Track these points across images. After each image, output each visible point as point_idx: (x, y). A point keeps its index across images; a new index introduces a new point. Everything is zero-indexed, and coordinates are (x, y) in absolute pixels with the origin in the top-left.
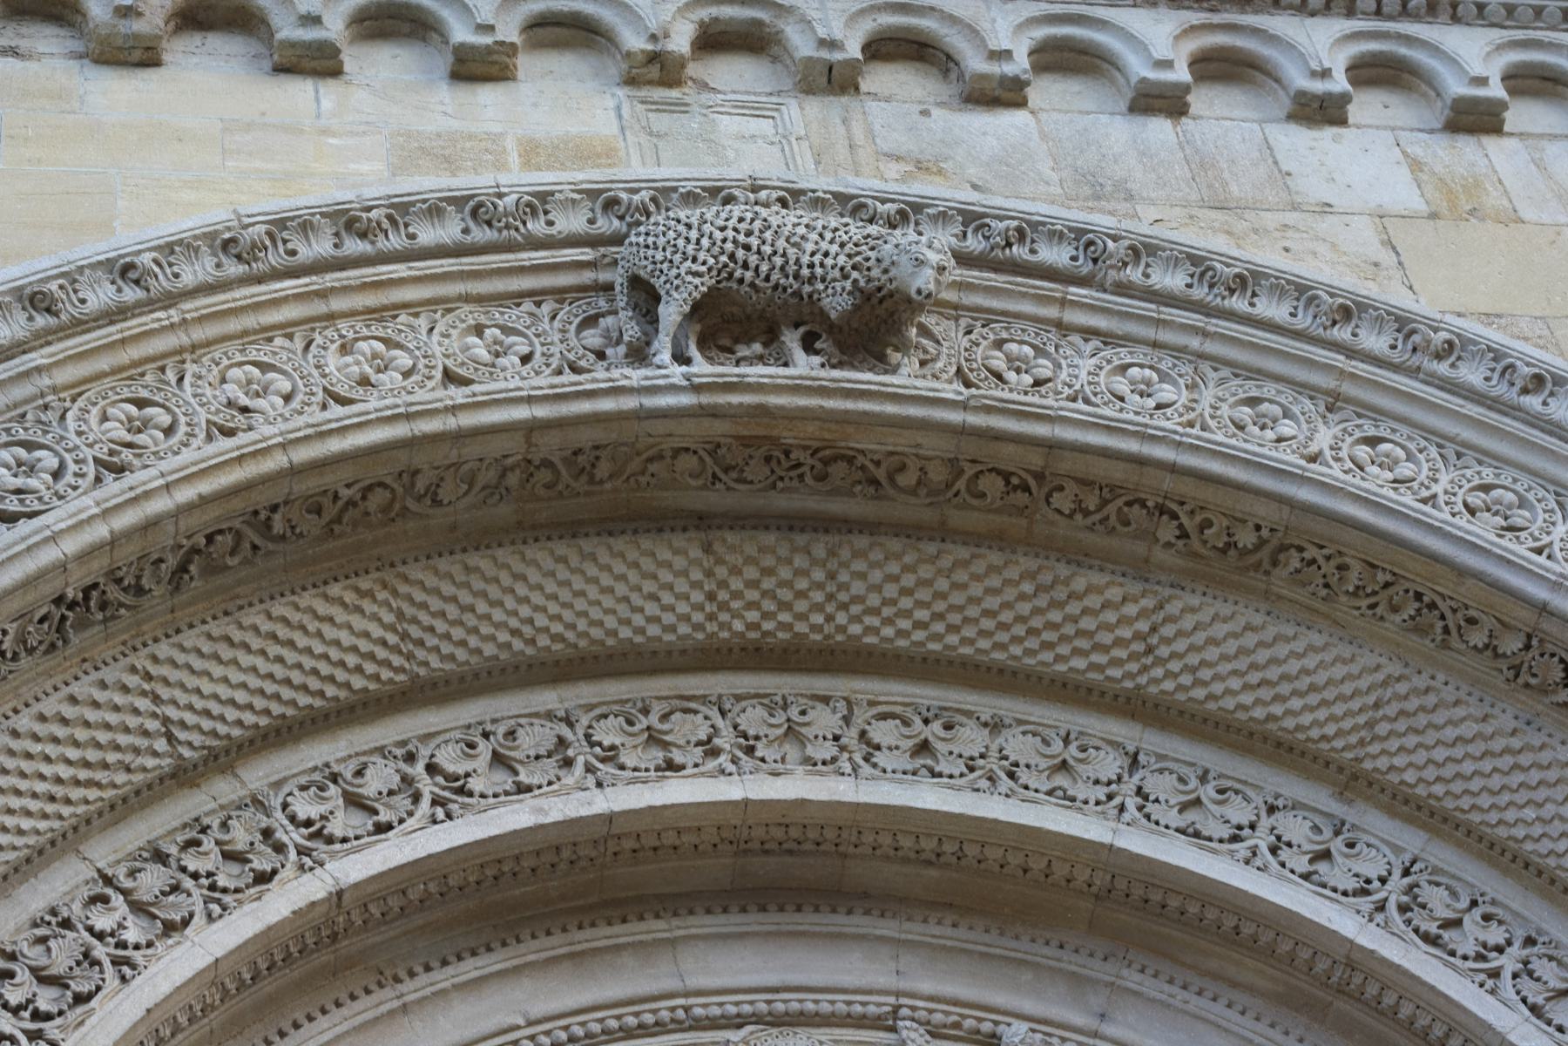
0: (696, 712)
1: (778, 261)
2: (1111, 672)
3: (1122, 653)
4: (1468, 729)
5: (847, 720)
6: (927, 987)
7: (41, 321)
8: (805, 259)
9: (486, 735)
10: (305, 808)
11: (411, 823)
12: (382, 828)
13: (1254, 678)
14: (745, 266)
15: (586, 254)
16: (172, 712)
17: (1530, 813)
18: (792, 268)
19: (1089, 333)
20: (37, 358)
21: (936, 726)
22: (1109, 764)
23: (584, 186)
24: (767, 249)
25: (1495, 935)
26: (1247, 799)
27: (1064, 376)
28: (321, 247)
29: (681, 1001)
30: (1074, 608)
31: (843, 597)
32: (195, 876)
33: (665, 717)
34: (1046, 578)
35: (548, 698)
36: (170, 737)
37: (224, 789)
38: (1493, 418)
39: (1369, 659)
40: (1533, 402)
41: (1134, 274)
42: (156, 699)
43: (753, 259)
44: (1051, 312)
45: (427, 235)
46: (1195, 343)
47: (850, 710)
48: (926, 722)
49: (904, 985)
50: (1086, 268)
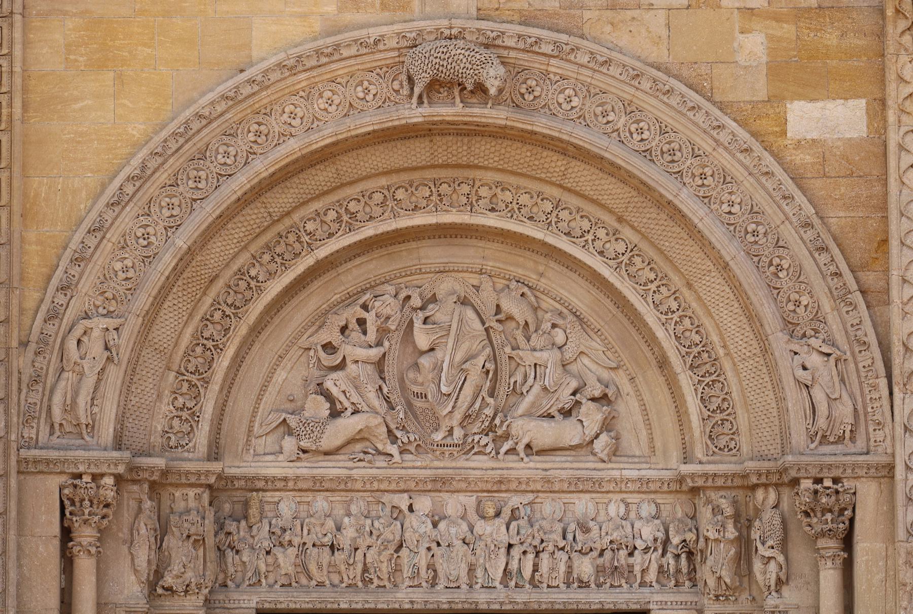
0: (426, 185)
1: (452, 71)
2: (552, 179)
3: (556, 175)
4: (654, 215)
5: (473, 186)
7: (230, 103)
8: (460, 71)
9: (363, 196)
10: (310, 226)
11: (340, 233)
12: (331, 235)
13: (594, 188)
14: (442, 72)
15: (396, 53)
16: (271, 210)
17: (667, 244)
18: (456, 73)
19: (555, 74)
20: (228, 116)
21: (499, 189)
22: (548, 206)
23: (396, 31)
24: (449, 67)
25: (652, 276)
26: (590, 221)
27: (543, 96)
28: (313, 62)
29: (419, 267)
30: (542, 161)
31: (473, 153)
32: (278, 255)
35: (383, 181)
36: (270, 216)
37: (287, 222)
38: (677, 116)
40: (690, 114)
41: (572, 57)
42: (266, 207)
43: (444, 71)
45: (346, 53)
47: (474, 183)
48: (497, 187)
49: (484, 263)
50: (555, 53)
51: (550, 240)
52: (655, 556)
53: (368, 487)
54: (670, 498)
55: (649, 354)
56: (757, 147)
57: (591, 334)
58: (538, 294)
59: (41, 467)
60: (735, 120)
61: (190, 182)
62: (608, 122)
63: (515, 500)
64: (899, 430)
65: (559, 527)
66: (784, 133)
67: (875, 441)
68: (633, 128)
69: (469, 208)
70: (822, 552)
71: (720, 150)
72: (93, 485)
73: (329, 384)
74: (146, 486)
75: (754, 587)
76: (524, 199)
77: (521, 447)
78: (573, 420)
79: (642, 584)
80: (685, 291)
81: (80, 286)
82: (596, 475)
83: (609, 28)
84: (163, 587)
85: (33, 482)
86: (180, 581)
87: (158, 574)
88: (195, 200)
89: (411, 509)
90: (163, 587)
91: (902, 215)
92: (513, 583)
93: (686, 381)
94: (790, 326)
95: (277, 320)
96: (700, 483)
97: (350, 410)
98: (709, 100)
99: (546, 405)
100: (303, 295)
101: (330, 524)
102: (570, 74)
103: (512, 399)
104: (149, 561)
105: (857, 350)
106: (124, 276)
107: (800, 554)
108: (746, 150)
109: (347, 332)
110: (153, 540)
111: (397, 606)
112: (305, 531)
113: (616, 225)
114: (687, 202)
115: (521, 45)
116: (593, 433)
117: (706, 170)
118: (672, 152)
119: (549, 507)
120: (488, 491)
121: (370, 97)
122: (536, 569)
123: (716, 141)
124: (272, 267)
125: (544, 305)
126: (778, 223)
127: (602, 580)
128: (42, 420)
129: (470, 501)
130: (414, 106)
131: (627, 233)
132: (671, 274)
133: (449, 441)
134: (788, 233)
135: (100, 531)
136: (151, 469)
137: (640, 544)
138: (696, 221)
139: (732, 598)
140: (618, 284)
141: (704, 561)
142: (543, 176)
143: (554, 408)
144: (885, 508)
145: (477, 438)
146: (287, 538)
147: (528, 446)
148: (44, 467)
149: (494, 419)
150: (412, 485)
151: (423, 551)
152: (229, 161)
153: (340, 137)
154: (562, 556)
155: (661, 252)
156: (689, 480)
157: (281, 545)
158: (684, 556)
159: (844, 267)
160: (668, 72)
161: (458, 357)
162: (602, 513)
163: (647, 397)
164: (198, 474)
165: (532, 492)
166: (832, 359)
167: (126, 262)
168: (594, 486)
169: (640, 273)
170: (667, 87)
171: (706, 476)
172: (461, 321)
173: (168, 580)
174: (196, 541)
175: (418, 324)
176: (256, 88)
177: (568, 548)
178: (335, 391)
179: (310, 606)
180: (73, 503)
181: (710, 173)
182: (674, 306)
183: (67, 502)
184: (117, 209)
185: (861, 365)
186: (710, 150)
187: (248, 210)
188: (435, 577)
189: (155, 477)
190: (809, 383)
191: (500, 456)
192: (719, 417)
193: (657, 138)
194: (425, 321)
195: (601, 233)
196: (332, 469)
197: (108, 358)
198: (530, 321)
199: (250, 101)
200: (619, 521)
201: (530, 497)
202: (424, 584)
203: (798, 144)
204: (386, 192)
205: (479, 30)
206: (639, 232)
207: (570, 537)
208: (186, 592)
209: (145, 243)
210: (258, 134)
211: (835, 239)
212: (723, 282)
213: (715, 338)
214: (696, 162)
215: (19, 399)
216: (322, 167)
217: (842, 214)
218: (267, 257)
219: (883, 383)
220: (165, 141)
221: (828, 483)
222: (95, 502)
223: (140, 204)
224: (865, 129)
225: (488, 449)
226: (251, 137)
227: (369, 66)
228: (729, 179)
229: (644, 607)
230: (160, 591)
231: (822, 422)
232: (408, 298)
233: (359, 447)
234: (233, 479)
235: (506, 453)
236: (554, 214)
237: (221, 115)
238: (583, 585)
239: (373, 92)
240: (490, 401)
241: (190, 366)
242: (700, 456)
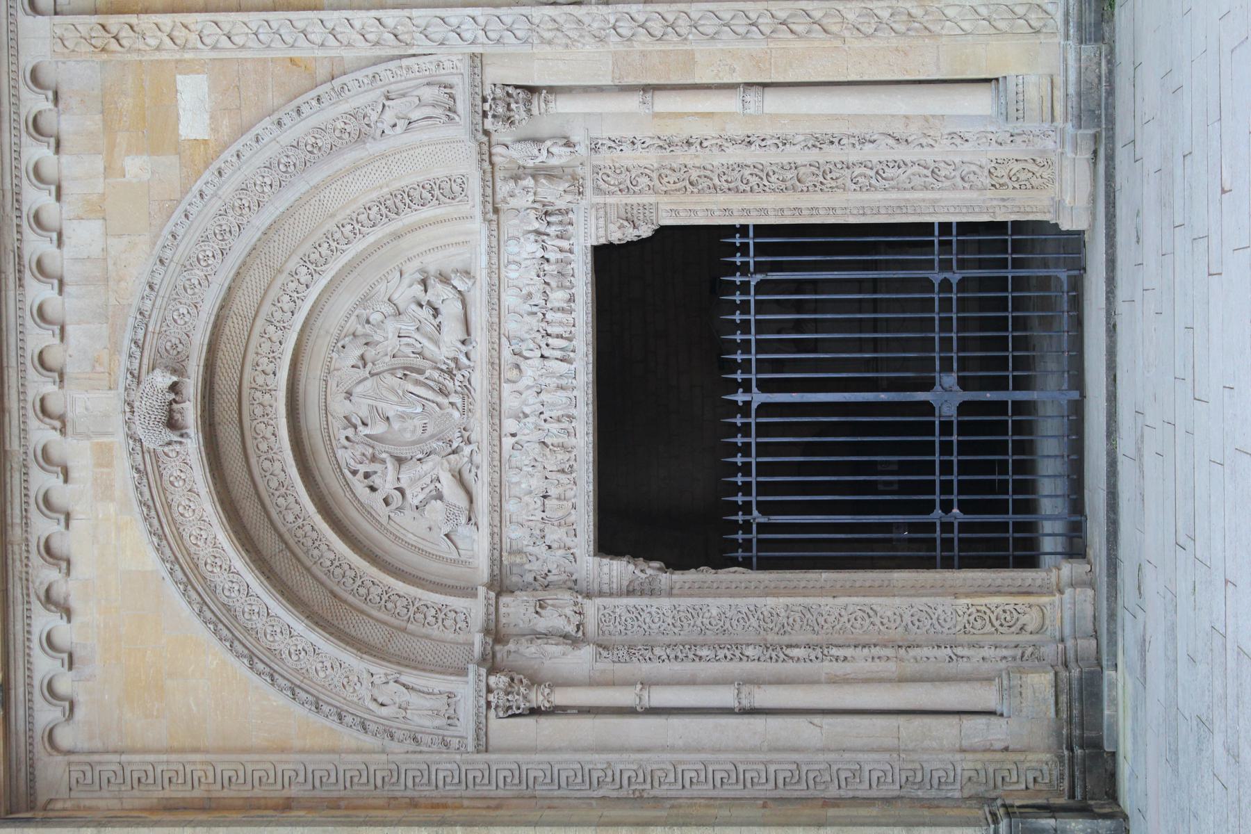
6: (319, 373)
10: (291, 518)
12: (297, 502)
19: (161, 326)
20: (200, 589)
25: (326, 245)
28: (155, 522)
33: (258, 434)
34: (227, 341)
35: (253, 460)
37: (287, 536)
39: (255, 266)
40: (191, 218)
44: (156, 336)
45: (147, 495)
46: (166, 299)
51: (298, 327)
52: (549, 242)
53: (497, 469)
54: (504, 228)
55: (389, 247)
56: (218, 164)
57: (373, 292)
58: (343, 335)
59: (482, 733)
60: (196, 181)
61: (254, 618)
62: (200, 284)
63: (506, 353)
64: (443, 49)
65: (527, 319)
66: (205, 142)
68: (204, 264)
69: (273, 392)
70: (542, 111)
71: (220, 193)
72: (496, 692)
73: (416, 502)
74: (498, 648)
75: (572, 164)
76: (266, 347)
77: (464, 349)
78: (442, 308)
79: (571, 252)
80: (336, 220)
81: (338, 704)
82: (485, 288)
83: (123, 284)
84: (577, 632)
85: (493, 742)
86: (572, 619)
87: (566, 636)
88: (268, 614)
89: (513, 435)
90: (577, 632)
91: (269, 47)
92: (572, 354)
93: (408, 218)
94: (361, 137)
95: (367, 542)
96: (490, 207)
97: (437, 484)
98: (179, 202)
99: (430, 329)
100: (346, 522)
101: (526, 499)
102: (161, 315)
103: (427, 354)
104: (556, 644)
105: (379, 83)
106: (330, 669)
107: (545, 127)
108: (220, 173)
109: (375, 486)
110: (539, 641)
111: (591, 446)
112: (533, 518)
113: (285, 274)
114: (262, 220)
115: (138, 354)
116: (453, 291)
117: (236, 204)
118: (223, 232)
119: (511, 326)
120: (500, 374)
121: (183, 475)
122: (559, 336)
123: (213, 196)
124: (324, 547)
125: (351, 331)
126: (278, 146)
127: (568, 284)
128: (446, 733)
129: (506, 387)
130: (189, 441)
131: (292, 265)
132: (324, 230)
133: (460, 405)
134: (288, 137)
135: (533, 684)
136: (484, 644)
137: (540, 253)
138: (278, 213)
139: (581, 181)
140: (333, 273)
141: (552, 204)
142: (246, 333)
143: (433, 322)
145: (457, 383)
146: (538, 532)
147: (463, 342)
148: (482, 733)
149: (442, 370)
150: (496, 434)
151: (546, 426)
152: (237, 588)
153: (216, 499)
154: (549, 316)
155: (305, 238)
156: (488, 216)
157: (544, 537)
158: (548, 219)
159: (314, 93)
160: (157, 236)
161: (395, 399)
162: (515, 283)
163: (423, 248)
164: (488, 605)
165: (499, 339)
166: (387, 103)
167: (319, 668)
168: (495, 290)
169: (323, 255)
170: (170, 237)
171: (484, 203)
172: (364, 396)
173: (571, 629)
174: (541, 606)
175: (367, 431)
176: (177, 567)
177: (544, 311)
178: (421, 497)
179: (591, 514)
180: (510, 708)
181: (239, 201)
182: (350, 227)
183: (510, 712)
184: (276, 676)
185: (392, 80)
186: (220, 203)
187: (277, 570)
188: (569, 416)
189: (490, 640)
190: (407, 122)
191: (472, 364)
192: (437, 192)
193: (211, 244)
194: (365, 424)
195: (293, 286)
196: (483, 497)
197: (396, 682)
198: (365, 341)
199: (188, 571)
200: (522, 270)
201: (504, 340)
202: (573, 424)
203: (214, 130)
204: (262, 458)
205: (126, 389)
206: (290, 256)
207: (535, 309)
208: (580, 613)
209: (303, 653)
210: (214, 564)
211: (291, 100)
212: (328, 189)
213: (374, 195)
214: (230, 211)
215: (427, 752)
216: (241, 511)
217: (270, 95)
218: (316, 552)
219: (405, 62)
220: (221, 639)
221: (487, 107)
222: (510, 689)
223: (272, 658)
224: (201, 76)
225: (466, 374)
226: (217, 570)
227: (157, 476)
228: (244, 186)
229: (589, 249)
230: (580, 634)
231: (438, 112)
232: (347, 438)
233: (466, 475)
234: (492, 576)
235: (469, 359)
236: (278, 324)
237: (199, 595)
238: (572, 299)
239: (179, 473)
240: (427, 374)
241: (401, 614)
242: (468, 207)
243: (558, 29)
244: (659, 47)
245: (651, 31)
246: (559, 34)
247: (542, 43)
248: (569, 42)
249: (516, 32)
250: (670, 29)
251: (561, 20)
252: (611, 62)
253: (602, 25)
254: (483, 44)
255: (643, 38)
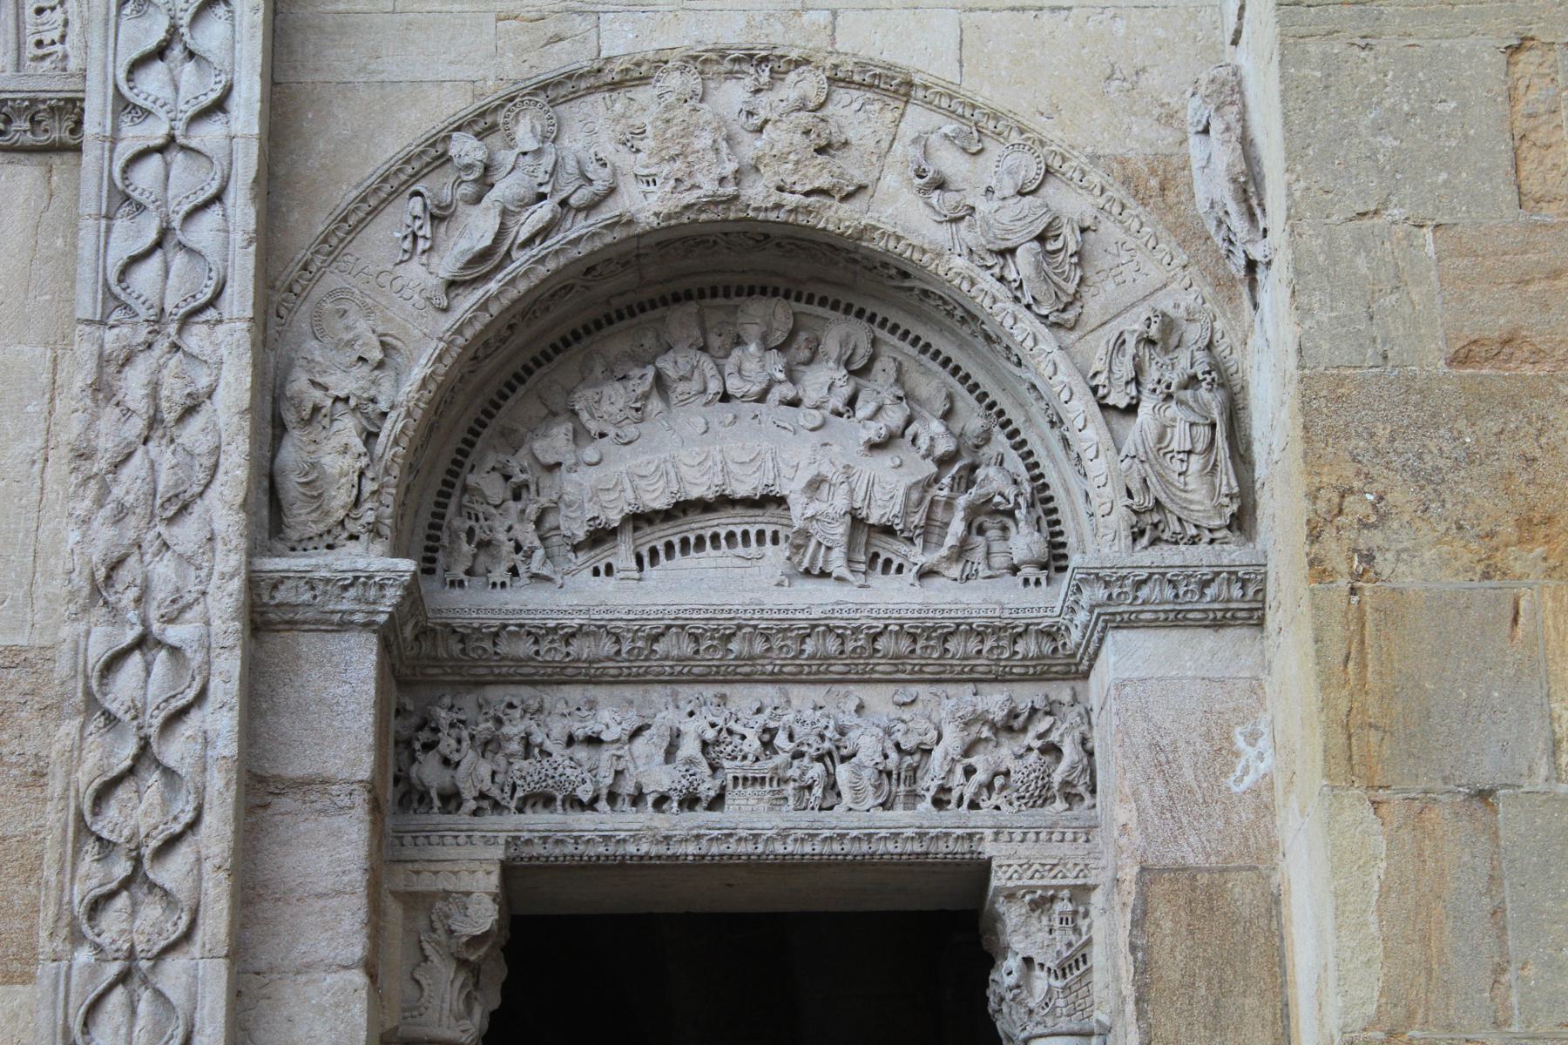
67: (39, 44)
144: (60, 242)
243: (154, 421)
244: (55, 819)
245: (123, 793)
246: (137, 425)
247: (103, 360)
248: (101, 464)
249: (156, 261)
250: (122, 869)
251: (193, 433)
252: (22, 641)
253: (161, 593)
254: (114, 140)
255: (91, 759)
